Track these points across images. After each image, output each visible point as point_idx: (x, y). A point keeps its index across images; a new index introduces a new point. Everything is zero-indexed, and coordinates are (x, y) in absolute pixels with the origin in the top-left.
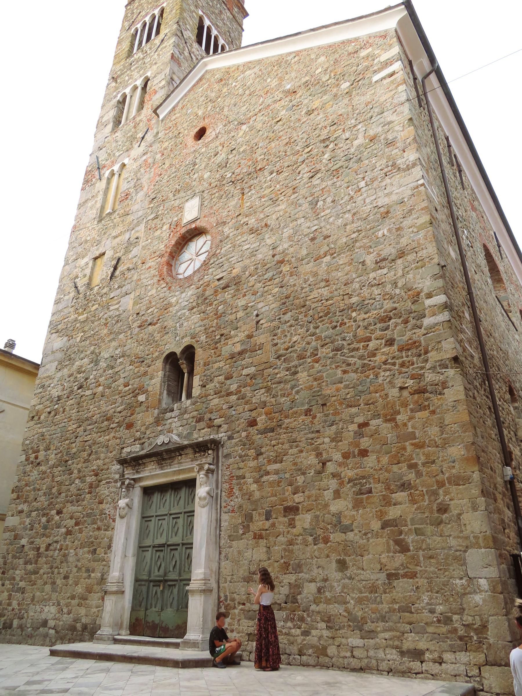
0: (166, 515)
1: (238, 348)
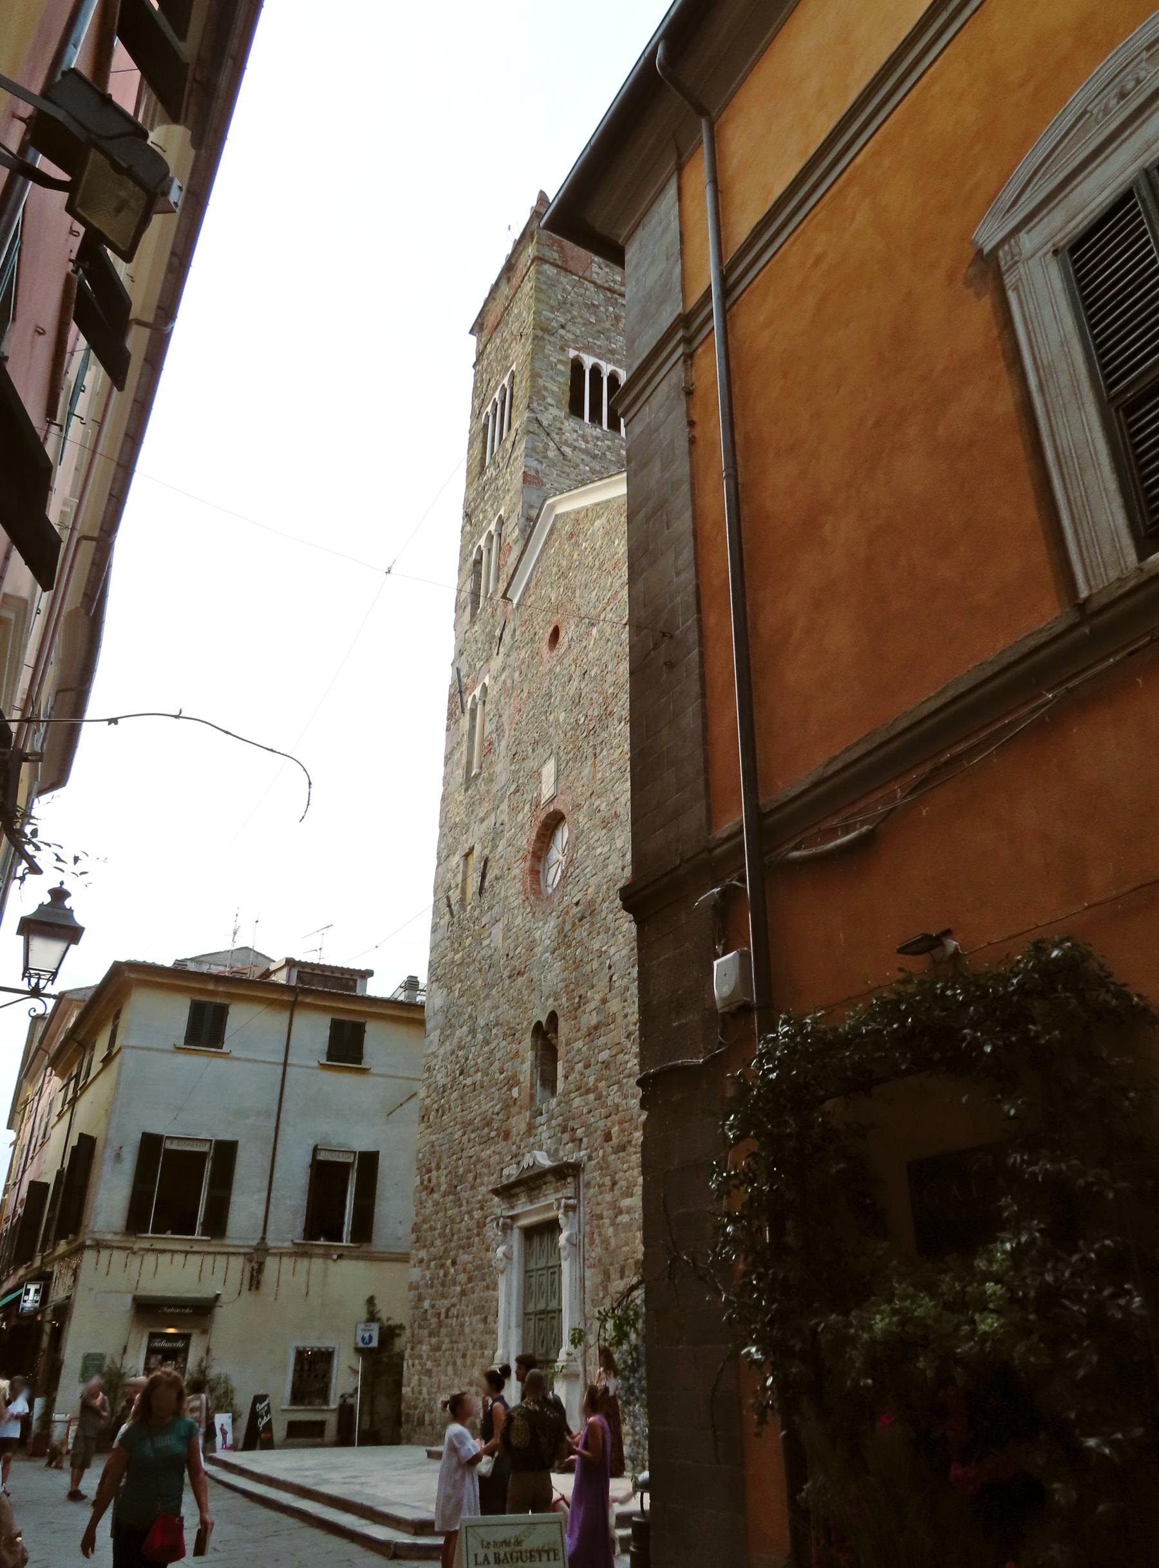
1: (594, 1022)
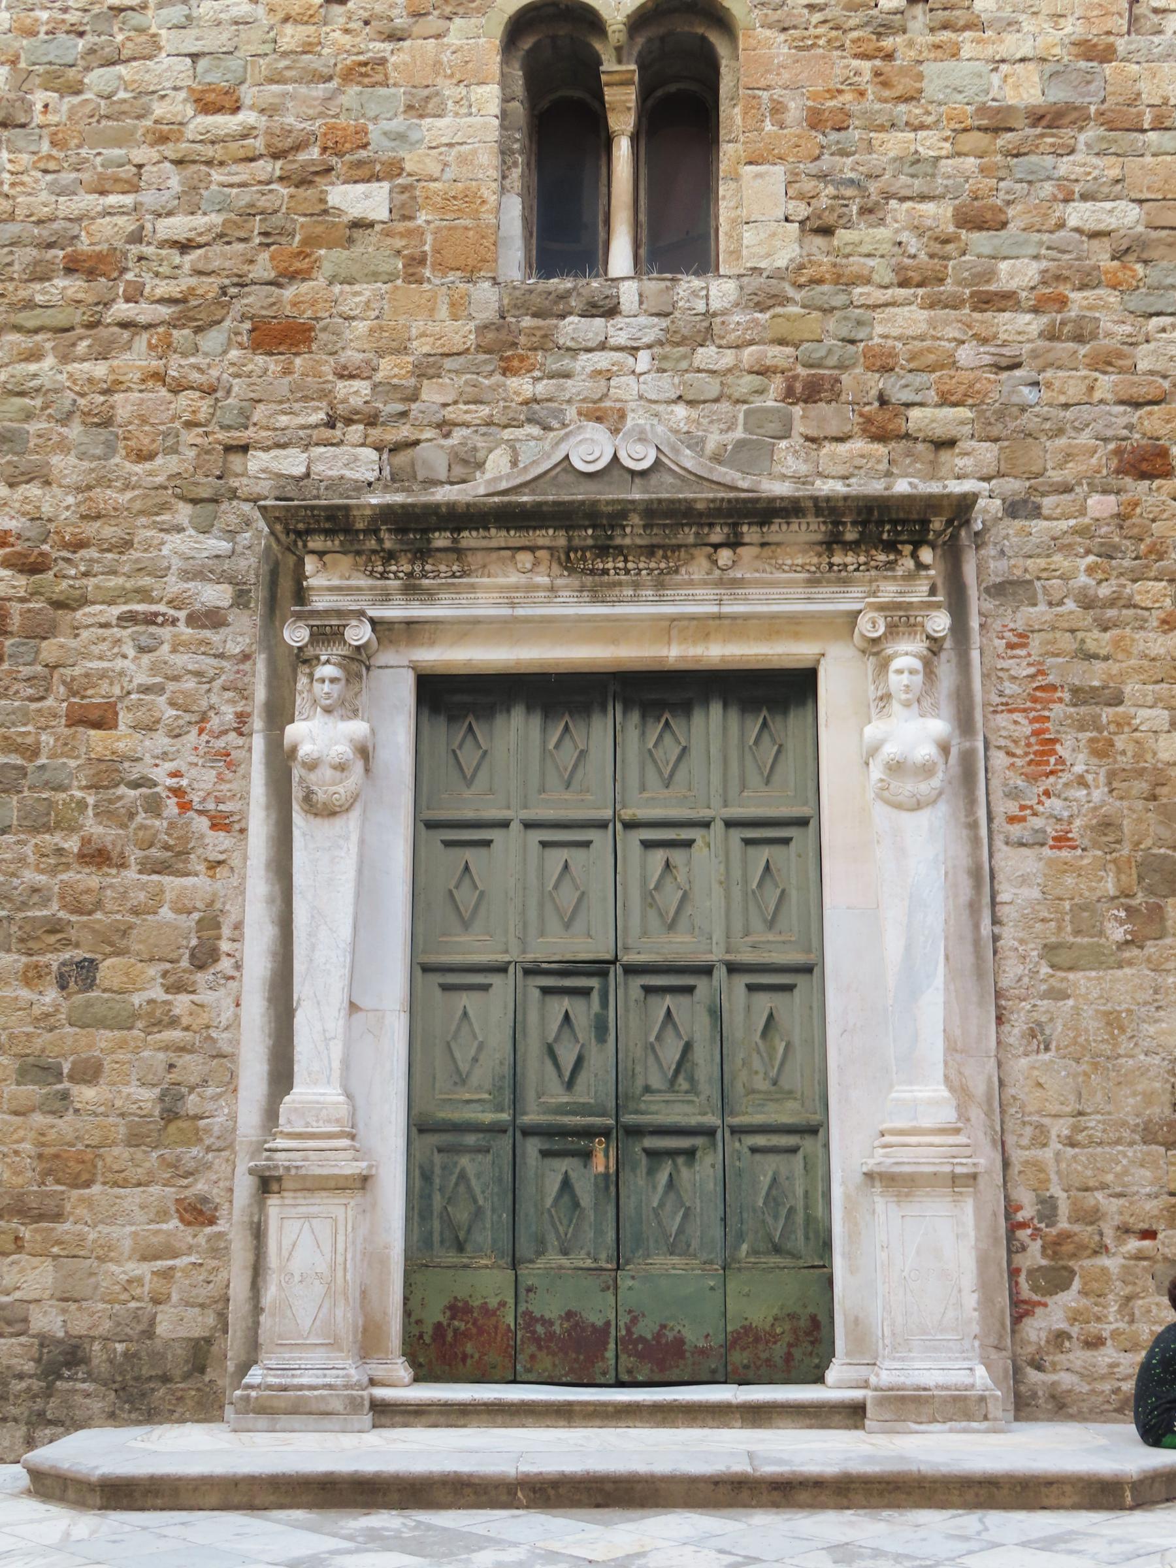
0: (602, 825)
1: (1026, 90)
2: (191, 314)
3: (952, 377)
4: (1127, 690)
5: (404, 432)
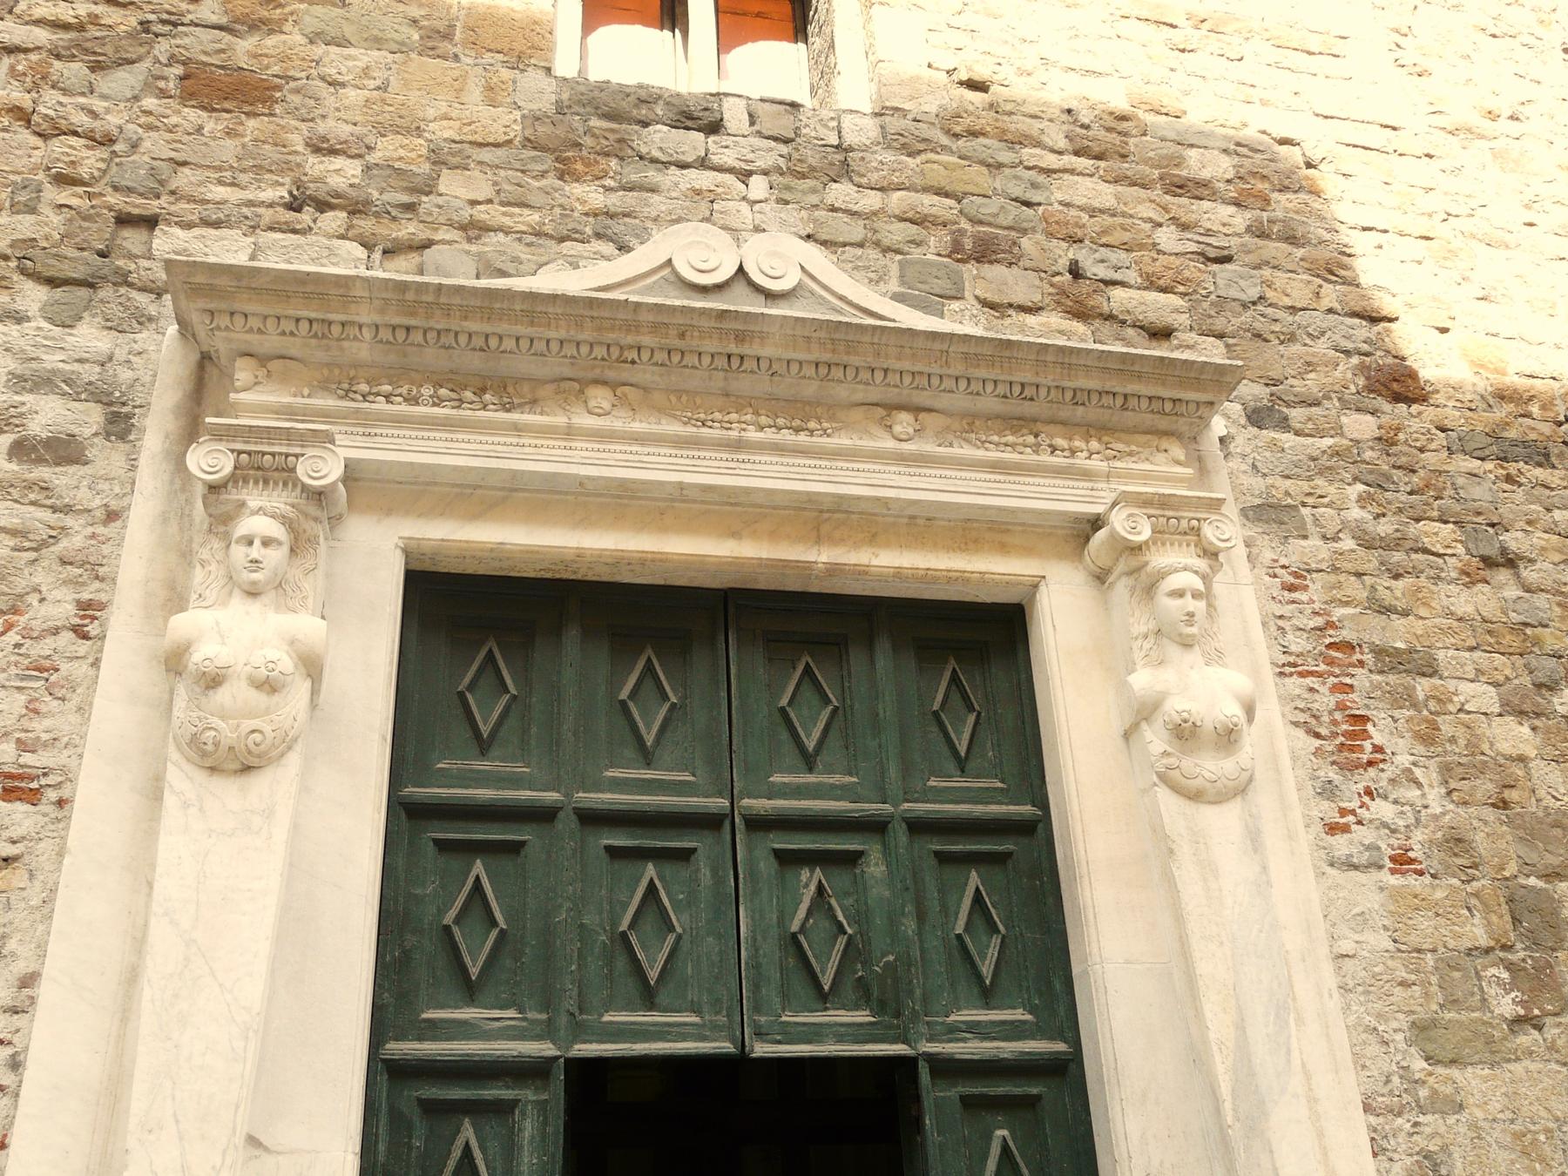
2: (88, 45)
3: (1155, 260)
4: (1441, 655)
5: (408, 229)
